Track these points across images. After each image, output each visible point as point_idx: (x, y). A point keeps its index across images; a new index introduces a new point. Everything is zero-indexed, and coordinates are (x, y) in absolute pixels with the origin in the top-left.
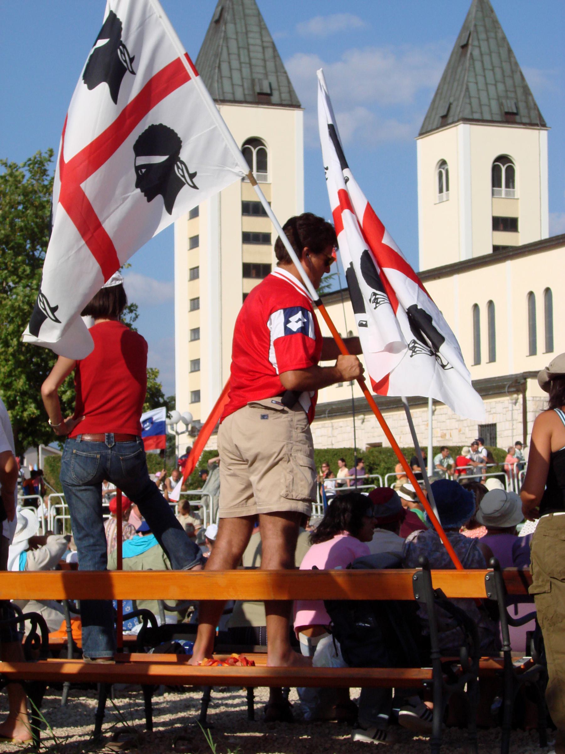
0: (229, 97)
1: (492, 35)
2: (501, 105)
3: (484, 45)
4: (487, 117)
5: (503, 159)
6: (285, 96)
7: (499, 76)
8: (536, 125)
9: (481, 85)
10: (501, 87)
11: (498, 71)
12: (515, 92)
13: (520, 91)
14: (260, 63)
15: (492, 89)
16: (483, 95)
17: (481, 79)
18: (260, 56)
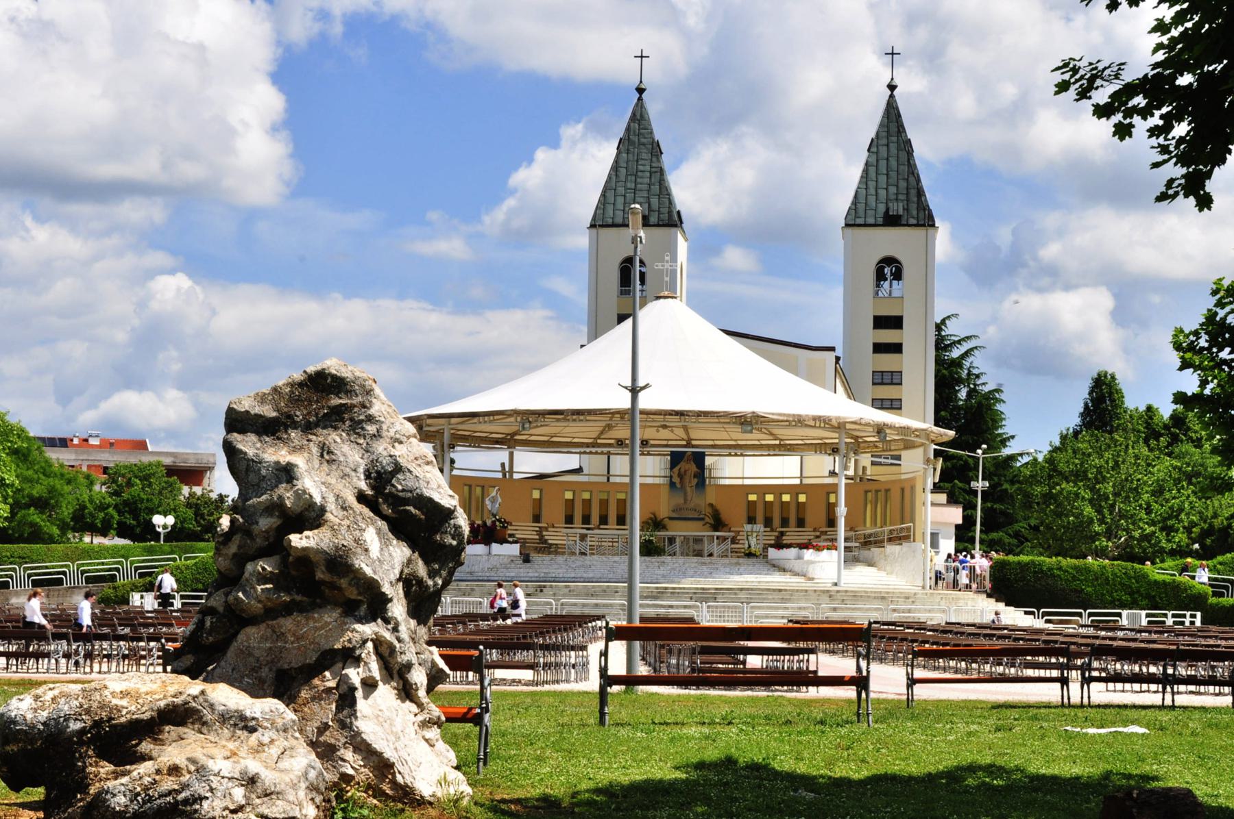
0: (610, 221)
1: (894, 139)
2: (887, 210)
3: (883, 150)
4: (871, 221)
5: (889, 261)
6: (665, 217)
7: (893, 180)
8: (924, 225)
9: (872, 191)
10: (893, 190)
11: (893, 174)
12: (907, 194)
13: (913, 192)
14: (646, 187)
15: (882, 193)
16: (872, 200)
17: (872, 184)
18: (647, 180)
